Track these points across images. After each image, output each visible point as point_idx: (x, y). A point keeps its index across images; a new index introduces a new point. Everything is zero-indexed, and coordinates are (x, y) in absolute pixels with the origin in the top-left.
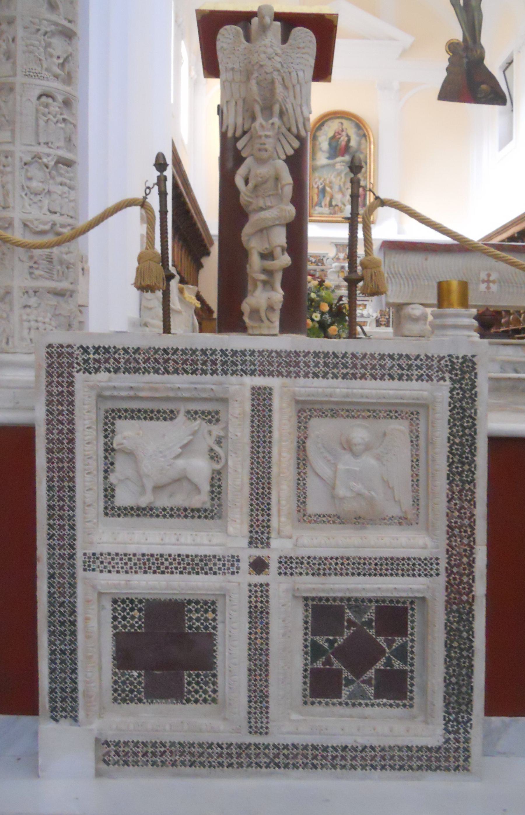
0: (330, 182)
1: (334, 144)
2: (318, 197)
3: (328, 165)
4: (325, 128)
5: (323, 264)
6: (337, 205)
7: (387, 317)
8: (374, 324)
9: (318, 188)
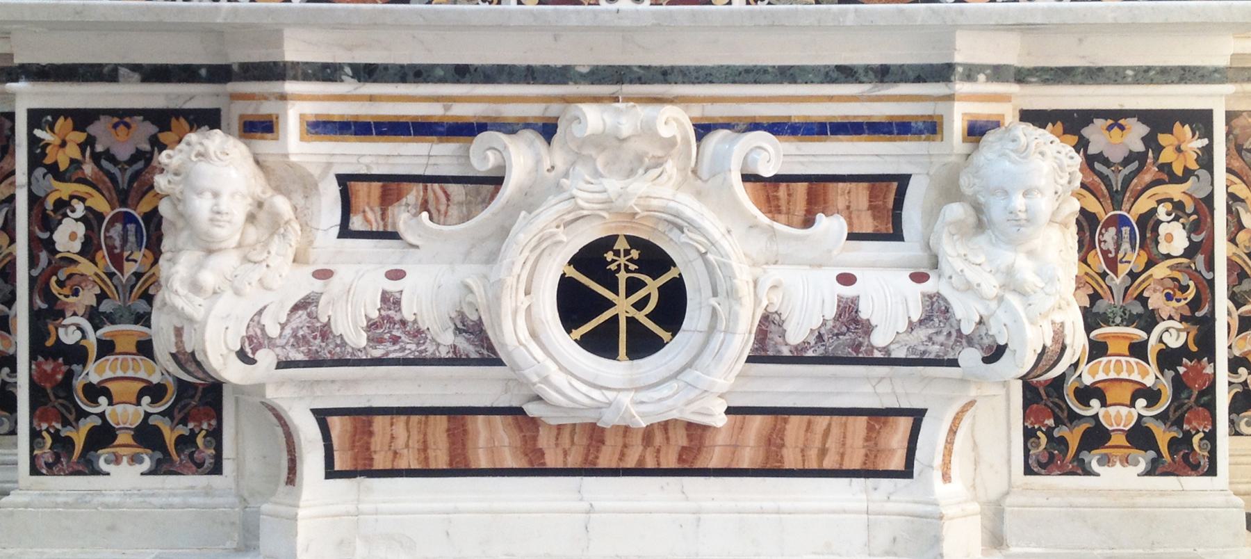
7: (1174, 335)
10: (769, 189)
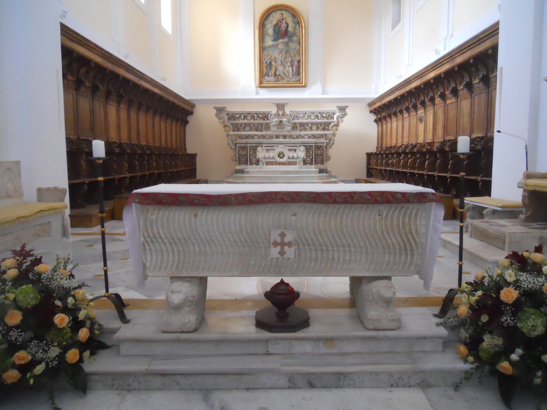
0: (275, 58)
1: (277, 30)
2: (266, 69)
3: (273, 46)
4: (271, 18)
5: (268, 119)
6: (279, 75)
7: (311, 158)
8: (302, 163)
9: (266, 62)
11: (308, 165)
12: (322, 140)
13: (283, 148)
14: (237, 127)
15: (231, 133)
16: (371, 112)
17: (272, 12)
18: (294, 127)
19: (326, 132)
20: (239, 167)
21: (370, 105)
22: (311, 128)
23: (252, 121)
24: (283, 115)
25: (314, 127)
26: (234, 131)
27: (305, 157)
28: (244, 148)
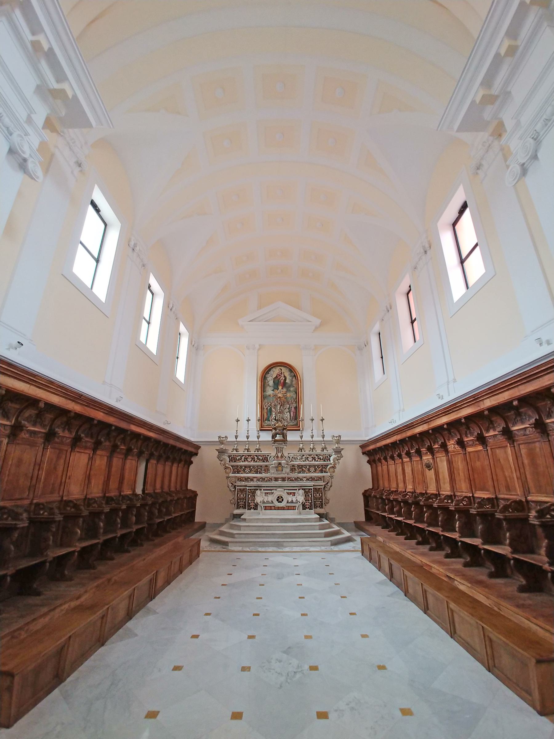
4: (271, 372)
5: (267, 461)
8: (301, 507)
9: (267, 409)
10: (288, 493)
11: (308, 510)
12: (321, 483)
13: (282, 491)
14: (237, 470)
15: (231, 475)
16: (363, 453)
17: (272, 368)
18: (293, 469)
19: (324, 474)
20: (237, 512)
21: (362, 447)
22: (309, 470)
23: (252, 463)
24: (282, 457)
25: (312, 469)
26: (234, 473)
27: (304, 501)
28: (242, 491)
